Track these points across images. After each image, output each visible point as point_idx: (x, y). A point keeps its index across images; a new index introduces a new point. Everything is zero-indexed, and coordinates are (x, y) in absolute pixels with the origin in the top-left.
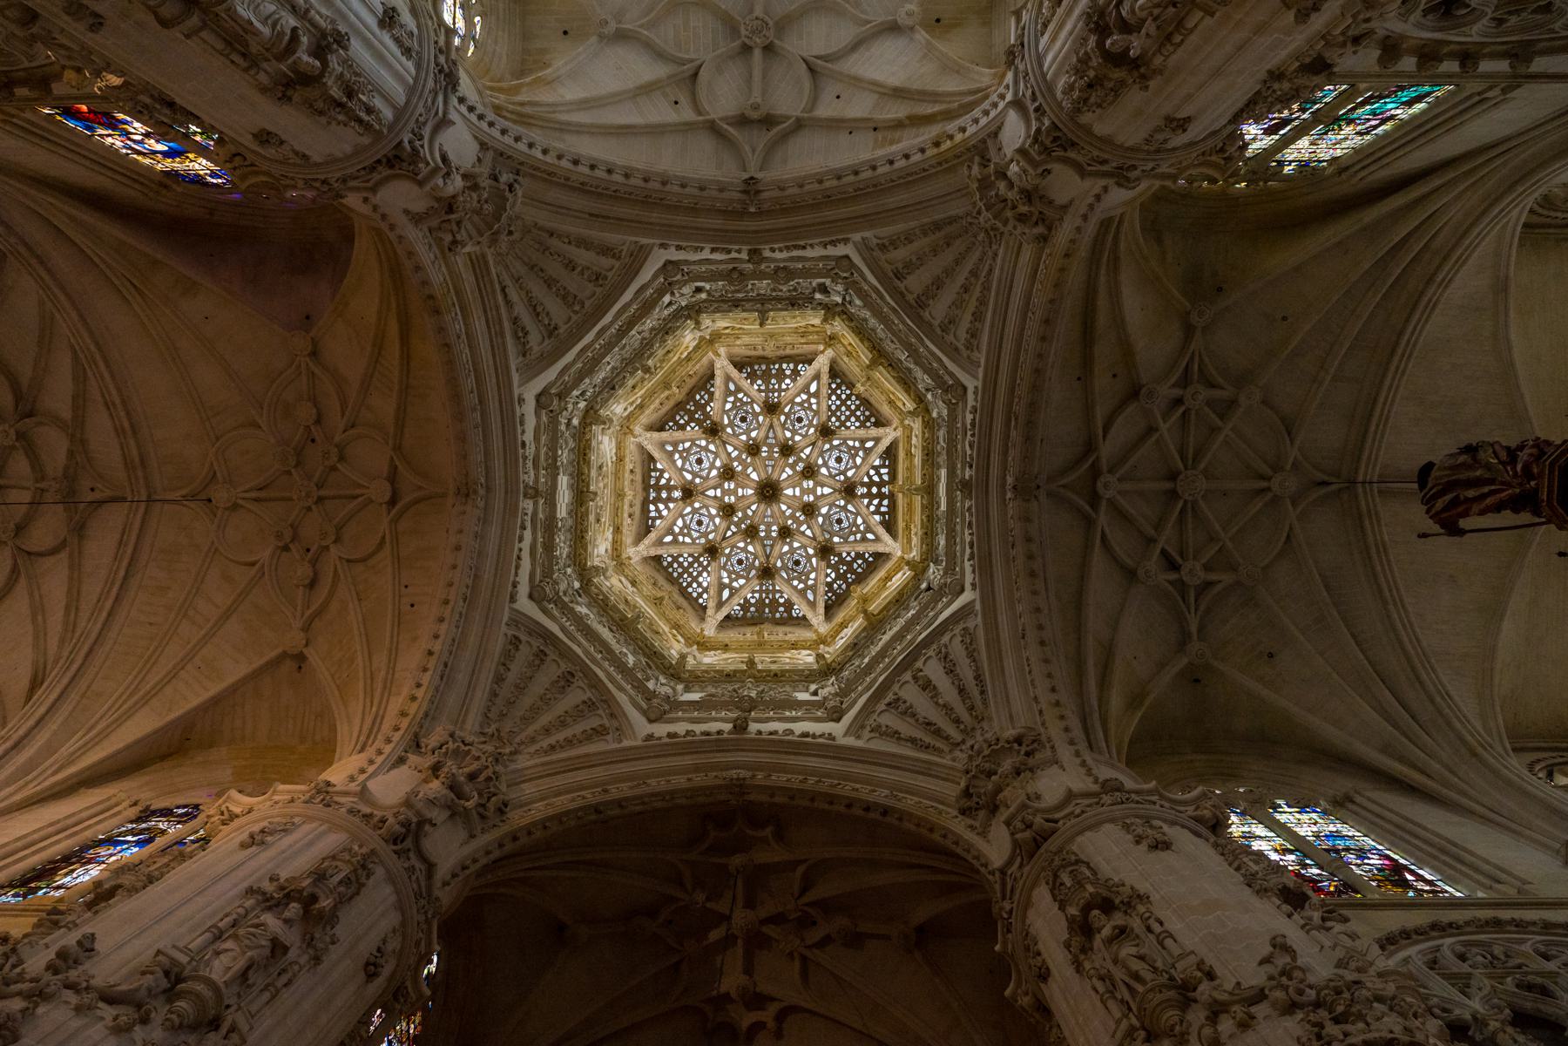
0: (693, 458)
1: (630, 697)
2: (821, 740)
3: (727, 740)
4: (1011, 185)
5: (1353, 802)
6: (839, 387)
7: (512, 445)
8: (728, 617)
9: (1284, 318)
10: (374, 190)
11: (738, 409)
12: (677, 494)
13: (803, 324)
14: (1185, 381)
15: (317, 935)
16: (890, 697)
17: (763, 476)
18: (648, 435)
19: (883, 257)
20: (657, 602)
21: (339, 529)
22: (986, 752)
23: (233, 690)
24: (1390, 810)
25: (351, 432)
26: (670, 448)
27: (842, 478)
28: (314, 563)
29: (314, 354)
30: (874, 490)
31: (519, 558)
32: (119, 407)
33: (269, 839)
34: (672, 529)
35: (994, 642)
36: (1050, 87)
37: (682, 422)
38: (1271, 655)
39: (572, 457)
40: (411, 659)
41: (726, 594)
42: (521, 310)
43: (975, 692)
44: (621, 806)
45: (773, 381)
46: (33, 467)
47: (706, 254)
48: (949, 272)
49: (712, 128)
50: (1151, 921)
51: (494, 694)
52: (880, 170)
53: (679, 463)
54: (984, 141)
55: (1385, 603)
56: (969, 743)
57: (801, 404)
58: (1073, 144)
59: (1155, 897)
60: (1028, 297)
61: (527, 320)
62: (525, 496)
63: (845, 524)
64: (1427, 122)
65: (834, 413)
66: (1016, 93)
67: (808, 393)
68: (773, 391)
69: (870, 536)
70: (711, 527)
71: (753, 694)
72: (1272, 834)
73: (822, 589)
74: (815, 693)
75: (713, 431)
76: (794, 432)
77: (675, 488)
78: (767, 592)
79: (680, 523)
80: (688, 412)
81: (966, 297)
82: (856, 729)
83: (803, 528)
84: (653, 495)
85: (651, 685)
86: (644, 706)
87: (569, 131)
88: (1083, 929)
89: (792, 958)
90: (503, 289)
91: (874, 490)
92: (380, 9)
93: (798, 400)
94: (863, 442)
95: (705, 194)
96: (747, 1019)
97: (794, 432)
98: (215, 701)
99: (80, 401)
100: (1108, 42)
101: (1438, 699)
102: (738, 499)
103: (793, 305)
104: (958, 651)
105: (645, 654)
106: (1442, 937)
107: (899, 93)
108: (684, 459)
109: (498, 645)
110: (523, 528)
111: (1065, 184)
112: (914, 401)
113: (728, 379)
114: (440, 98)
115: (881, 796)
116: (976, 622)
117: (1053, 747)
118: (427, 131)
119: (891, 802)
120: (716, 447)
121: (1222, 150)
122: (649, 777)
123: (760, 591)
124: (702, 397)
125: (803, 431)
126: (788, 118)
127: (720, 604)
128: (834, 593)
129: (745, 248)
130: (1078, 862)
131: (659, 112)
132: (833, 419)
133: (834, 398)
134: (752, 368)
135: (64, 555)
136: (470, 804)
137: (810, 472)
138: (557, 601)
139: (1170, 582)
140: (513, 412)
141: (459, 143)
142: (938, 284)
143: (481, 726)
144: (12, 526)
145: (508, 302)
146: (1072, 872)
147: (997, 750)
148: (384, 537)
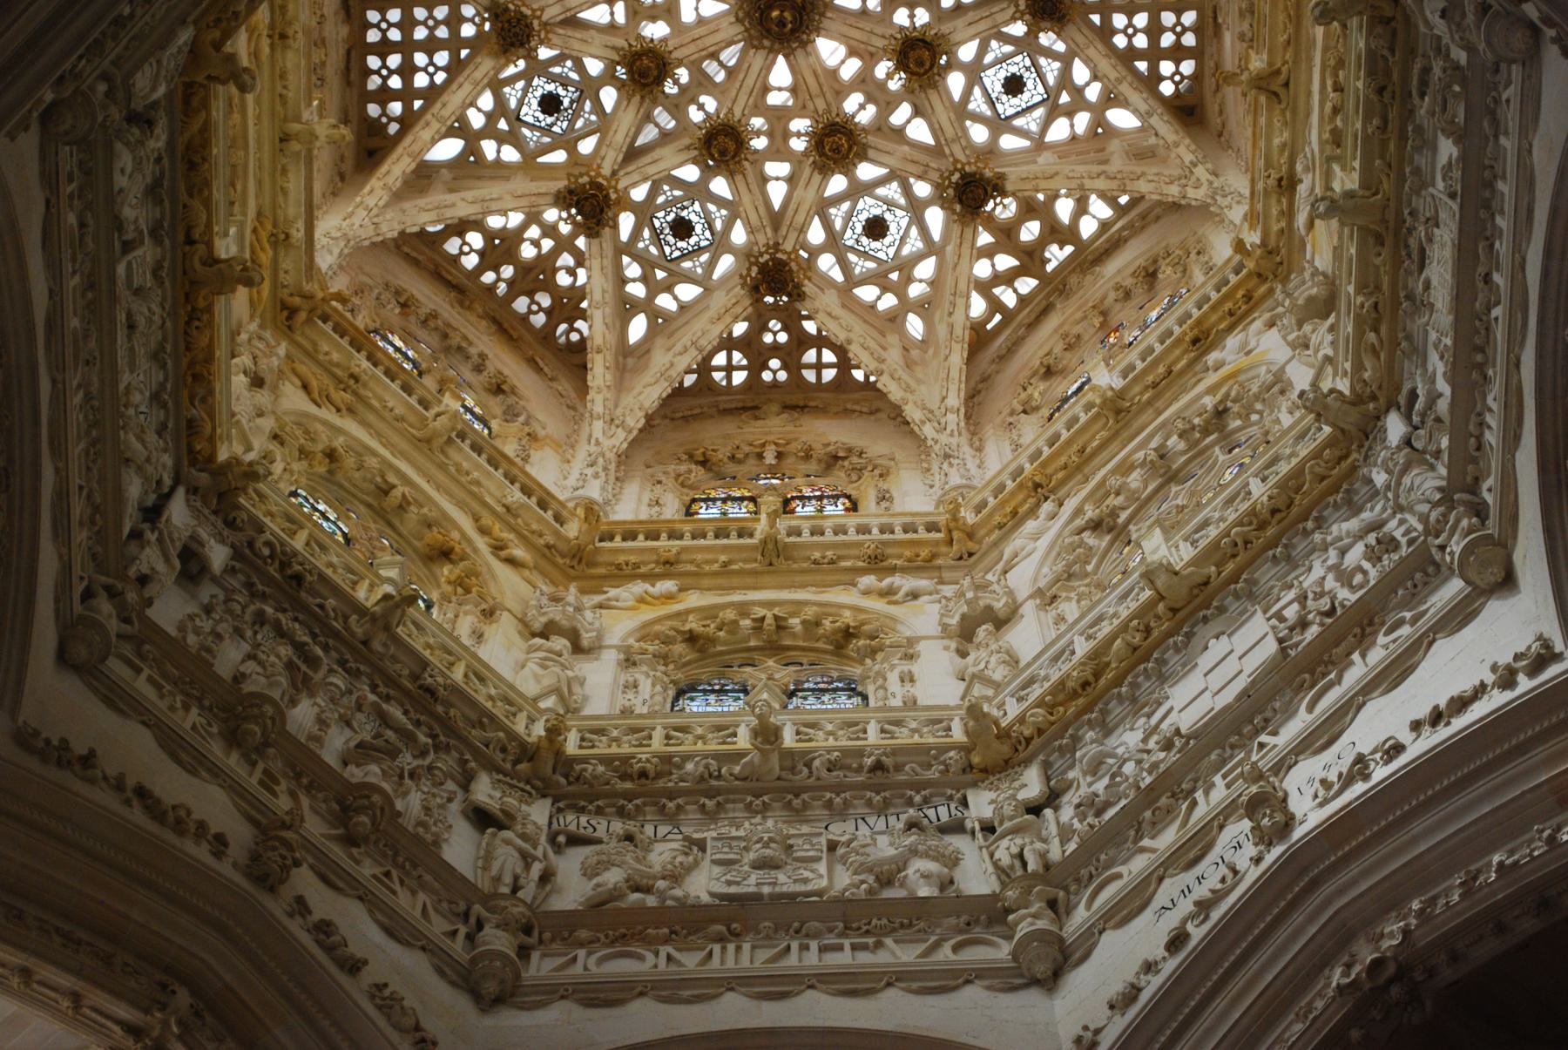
0: (884, 249)
6: (385, 95)
11: (669, 263)
13: (327, 414)
17: (758, 60)
18: (928, 431)
26: (915, 325)
31: (1437, 718)
34: (1092, 132)
37: (828, 356)
39: (1116, 710)
45: (527, 252)
53: (926, 269)
57: (512, 138)
65: (454, 43)
67: (472, 148)
68: (550, 230)
70: (997, 49)
76: (588, 88)
77: (991, 223)
79: (1059, 131)
80: (792, 362)
84: (1057, 255)
93: (510, 154)
97: (588, 88)
102: (870, 59)
103: (298, 579)
108: (906, 266)
110: (1360, 767)
112: (205, 105)
113: (629, 359)
120: (803, 229)
124: (729, 368)
129: (276, 907)
132: (468, 31)
133: (421, 80)
134: (551, 326)
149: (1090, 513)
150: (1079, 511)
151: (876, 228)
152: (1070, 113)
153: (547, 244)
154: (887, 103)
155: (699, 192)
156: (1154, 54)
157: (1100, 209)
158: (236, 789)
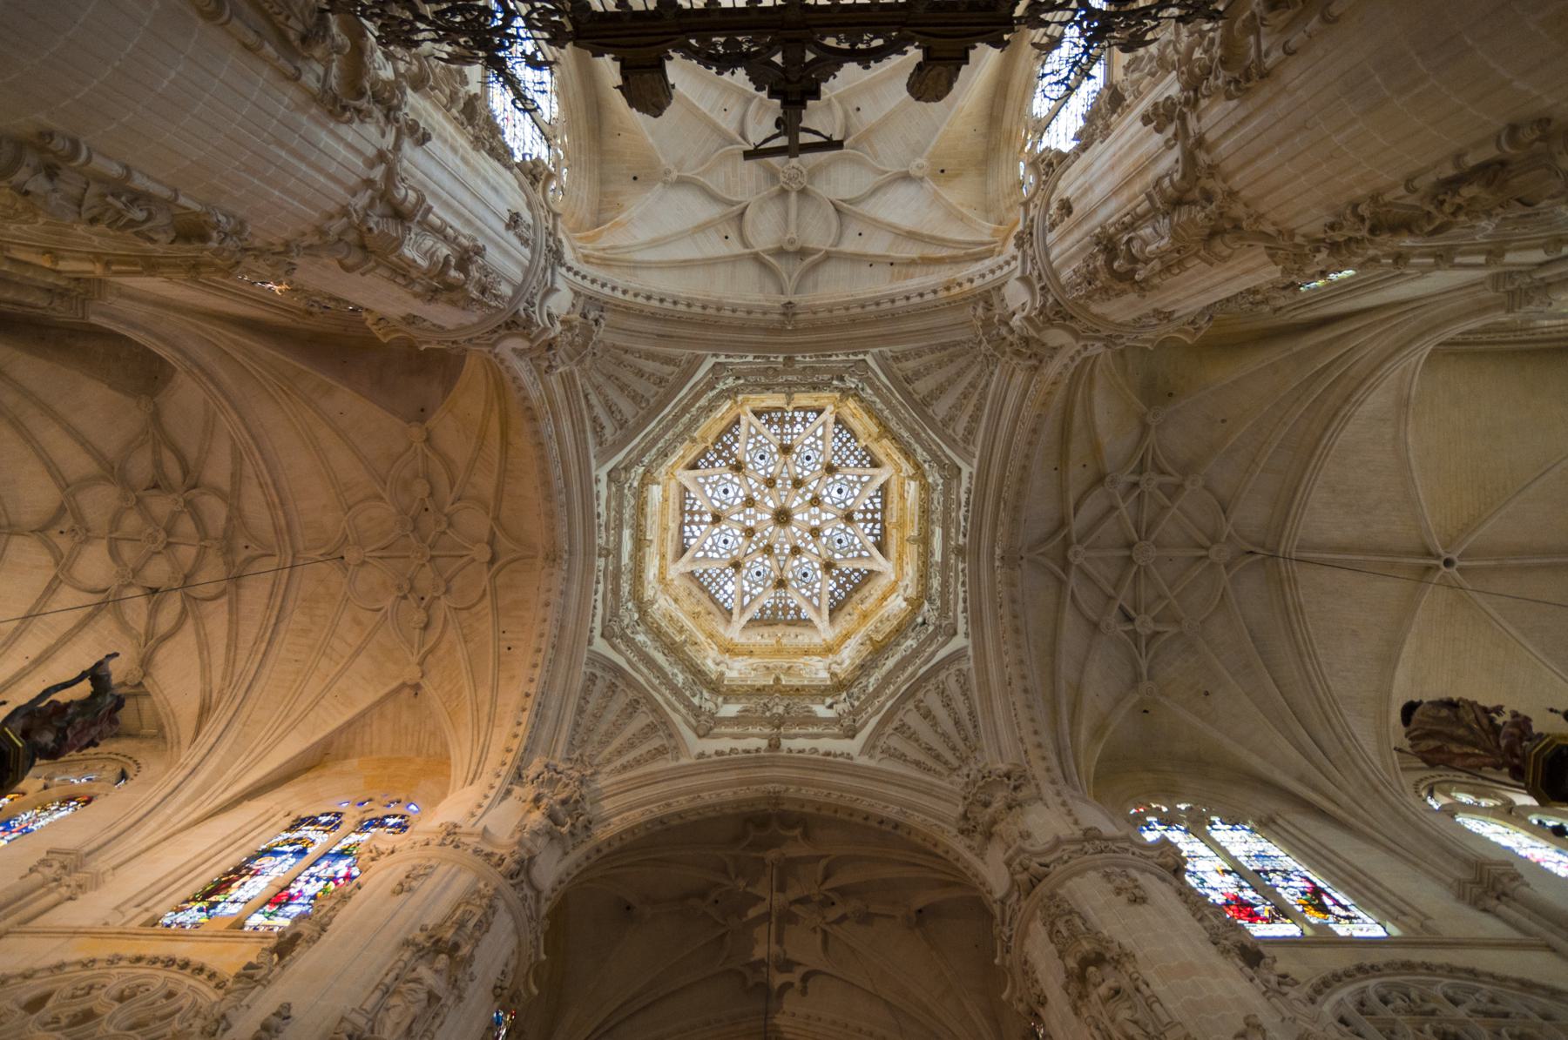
0: (721, 489)
1: (683, 716)
2: (840, 759)
3: (763, 757)
4: (1012, 331)
5: (1274, 822)
6: (840, 431)
7: (589, 515)
8: (750, 621)
9: (1223, 421)
10: (494, 345)
12: (708, 518)
14: (1141, 470)
15: (460, 976)
16: (896, 723)
17: (778, 504)
19: (895, 366)
20: (695, 616)
21: (448, 581)
22: (981, 783)
23: (363, 714)
24: (1307, 835)
25: (457, 505)
26: (701, 480)
27: (843, 506)
28: (427, 609)
29: (428, 440)
30: (869, 516)
31: (595, 607)
32: (271, 487)
33: (414, 884)
35: (984, 685)
36: (1055, 274)
38: (1207, 694)
40: (511, 698)
41: (747, 599)
42: (599, 411)
43: (969, 725)
44: (681, 818)
45: (787, 426)
46: (197, 527)
47: (750, 359)
48: (951, 382)
49: (756, 258)
50: (1140, 983)
51: (577, 724)
52: (898, 304)
53: (709, 493)
54: (988, 291)
55: (1301, 655)
56: (965, 770)
57: (809, 445)
58: (1072, 317)
59: (1139, 955)
60: (1019, 409)
61: (604, 418)
62: (600, 556)
63: (845, 543)
64: (1353, 284)
66: (1024, 271)
68: (787, 434)
69: (865, 553)
70: (735, 545)
71: (781, 710)
72: (1212, 854)
73: (826, 597)
74: (830, 707)
75: (738, 468)
76: (804, 468)
78: (780, 598)
79: (710, 541)
81: (965, 402)
82: (869, 748)
83: (811, 546)
84: (687, 518)
85: (696, 701)
86: (693, 721)
87: (641, 268)
88: (1079, 979)
89: (815, 932)
90: (586, 396)
91: (869, 516)
92: (507, 216)
93: (807, 442)
94: (860, 477)
95: (752, 316)
96: (778, 980)
97: (804, 468)
98: (350, 724)
99: (237, 478)
100: (1116, 265)
101: (1346, 741)
102: (758, 522)
104: (953, 687)
106: (1366, 979)
107: (912, 236)
108: (714, 490)
109: (578, 683)
110: (598, 582)
111: (1056, 336)
113: (750, 424)
114: (549, 271)
115: (892, 812)
116: (968, 665)
117: (1037, 785)
118: (537, 301)
119: (900, 818)
121: (1193, 322)
122: (702, 791)
123: (775, 598)
125: (811, 468)
126: (820, 251)
127: (743, 609)
128: (835, 599)
130: (1071, 912)
131: (714, 247)
135: (224, 599)
136: (565, 830)
137: (816, 501)
138: (624, 636)
139: (1126, 632)
140: (591, 489)
141: (560, 302)
142: (941, 390)
143: (568, 753)
144: (181, 576)
145: (590, 407)
146: (1067, 922)
147: (989, 781)
148: (485, 590)
155: (765, 468)
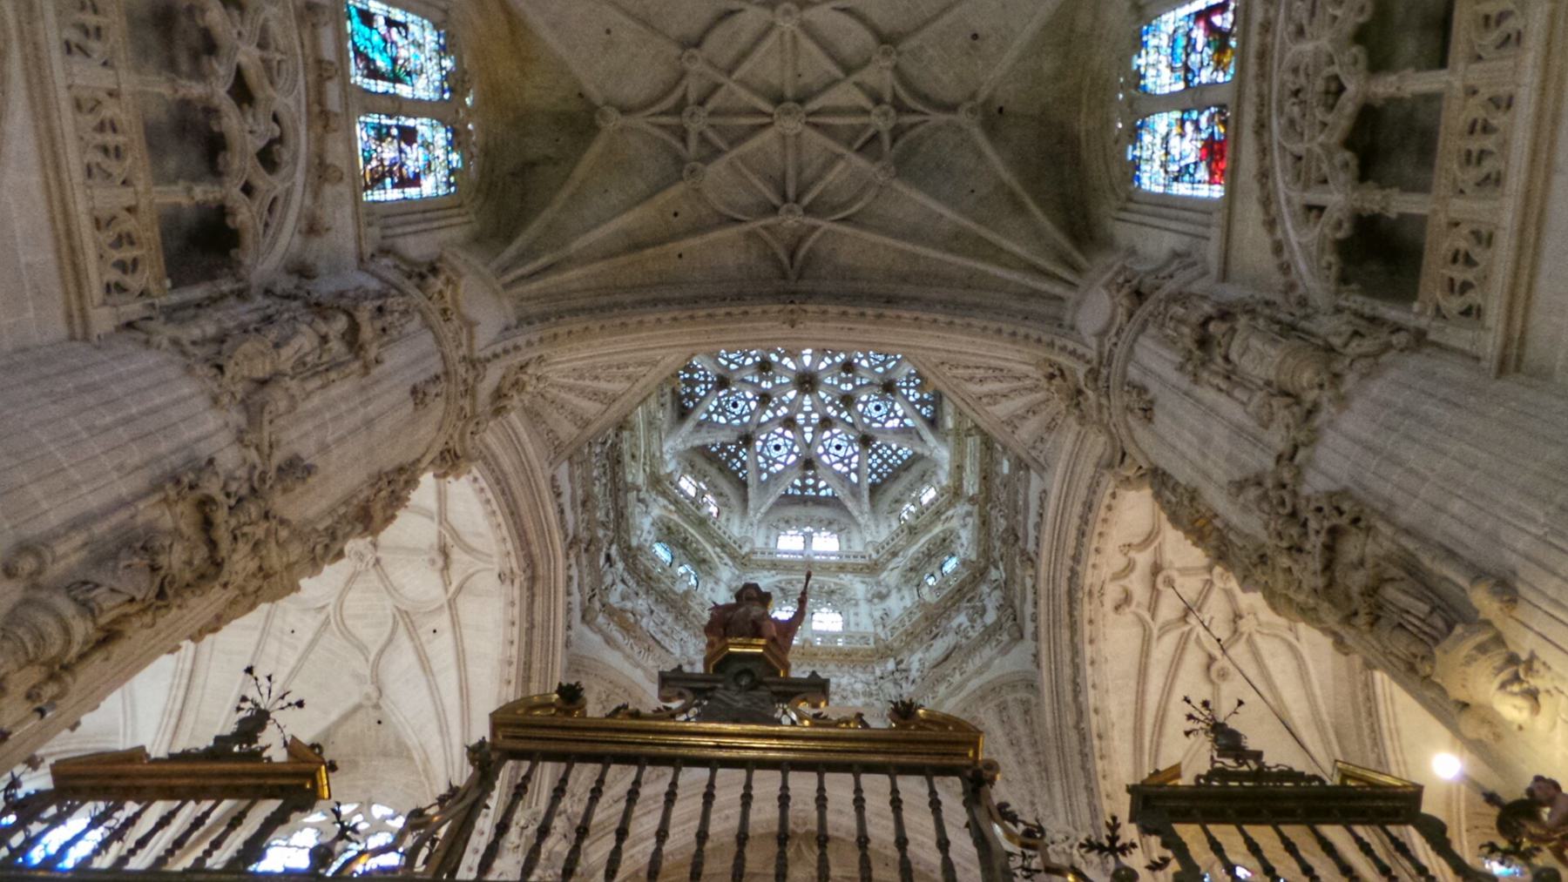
0: (775, 454)
9: (608, 32)
17: (791, 386)
18: (751, 513)
26: (764, 476)
34: (844, 474)
37: (739, 464)
38: (975, 37)
45: (696, 376)
53: (779, 467)
68: (706, 376)
75: (747, 440)
78: (908, 382)
79: (838, 467)
80: (728, 459)
84: (811, 492)
103: (619, 462)
105: (959, 601)
108: (776, 462)
123: (908, 388)
126: (440, 532)
131: (442, 650)
149: (783, 585)
150: (780, 582)
151: (777, 448)
152: (845, 465)
153: (702, 379)
154: (808, 423)
155: (748, 401)
156: (874, 471)
157: (829, 491)
158: (576, 523)
